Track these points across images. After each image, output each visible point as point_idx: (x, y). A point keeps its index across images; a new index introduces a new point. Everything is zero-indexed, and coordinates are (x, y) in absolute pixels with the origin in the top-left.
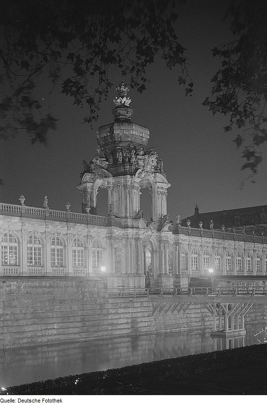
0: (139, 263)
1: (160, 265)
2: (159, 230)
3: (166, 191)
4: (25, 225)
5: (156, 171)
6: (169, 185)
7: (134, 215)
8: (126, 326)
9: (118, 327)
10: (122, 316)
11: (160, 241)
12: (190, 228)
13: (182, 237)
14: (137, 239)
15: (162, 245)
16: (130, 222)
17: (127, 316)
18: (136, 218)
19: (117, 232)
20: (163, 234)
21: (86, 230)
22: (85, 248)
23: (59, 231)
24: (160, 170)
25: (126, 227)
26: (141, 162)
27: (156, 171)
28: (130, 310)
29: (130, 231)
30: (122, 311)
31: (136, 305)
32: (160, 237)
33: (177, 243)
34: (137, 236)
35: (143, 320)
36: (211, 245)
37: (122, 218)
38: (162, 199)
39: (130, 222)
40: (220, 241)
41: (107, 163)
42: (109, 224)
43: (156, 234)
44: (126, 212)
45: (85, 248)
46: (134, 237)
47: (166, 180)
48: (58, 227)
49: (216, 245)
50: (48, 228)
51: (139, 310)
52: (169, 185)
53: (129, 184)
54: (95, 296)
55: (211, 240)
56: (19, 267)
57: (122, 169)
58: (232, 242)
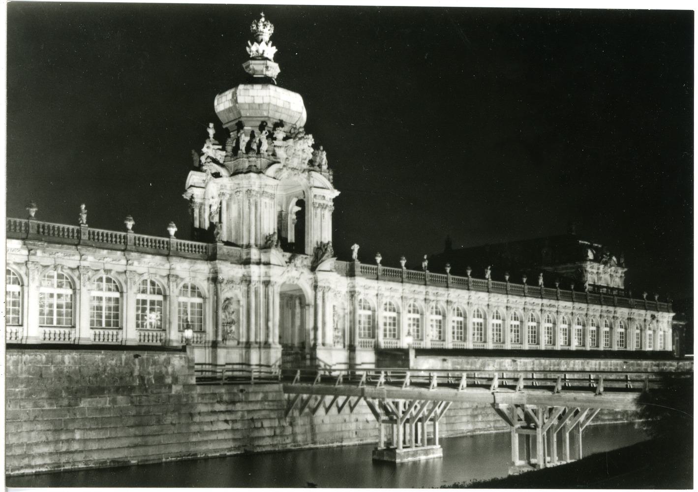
0: (270, 324)
1: (315, 328)
2: (313, 269)
3: (331, 203)
4: (35, 254)
5: (312, 168)
6: (337, 193)
7: (261, 242)
8: (229, 436)
9: (213, 437)
10: (222, 417)
11: (315, 287)
12: (380, 267)
13: (361, 282)
14: (267, 283)
15: (320, 294)
16: (255, 254)
17: (233, 417)
18: (266, 246)
19: (229, 271)
20: (320, 276)
21: (167, 266)
22: (165, 297)
23: (108, 267)
24: (320, 166)
25: (247, 262)
26: (281, 153)
27: (312, 168)
28: (239, 406)
29: (256, 272)
30: (222, 407)
31: (252, 398)
32: (316, 281)
33: (352, 294)
34: (267, 279)
35: (266, 424)
36: (422, 297)
37: (242, 246)
38: (323, 216)
39: (255, 254)
40: (441, 290)
41: (224, 153)
42: (211, 257)
43: (307, 275)
44: (249, 238)
45: (165, 297)
46: (262, 279)
47: (329, 185)
48: (106, 259)
49: (431, 297)
50: (85, 260)
51: (258, 407)
52: (337, 193)
53: (255, 188)
54: (169, 380)
55: (422, 288)
56: (20, 329)
57: (245, 163)
58: (464, 294)
